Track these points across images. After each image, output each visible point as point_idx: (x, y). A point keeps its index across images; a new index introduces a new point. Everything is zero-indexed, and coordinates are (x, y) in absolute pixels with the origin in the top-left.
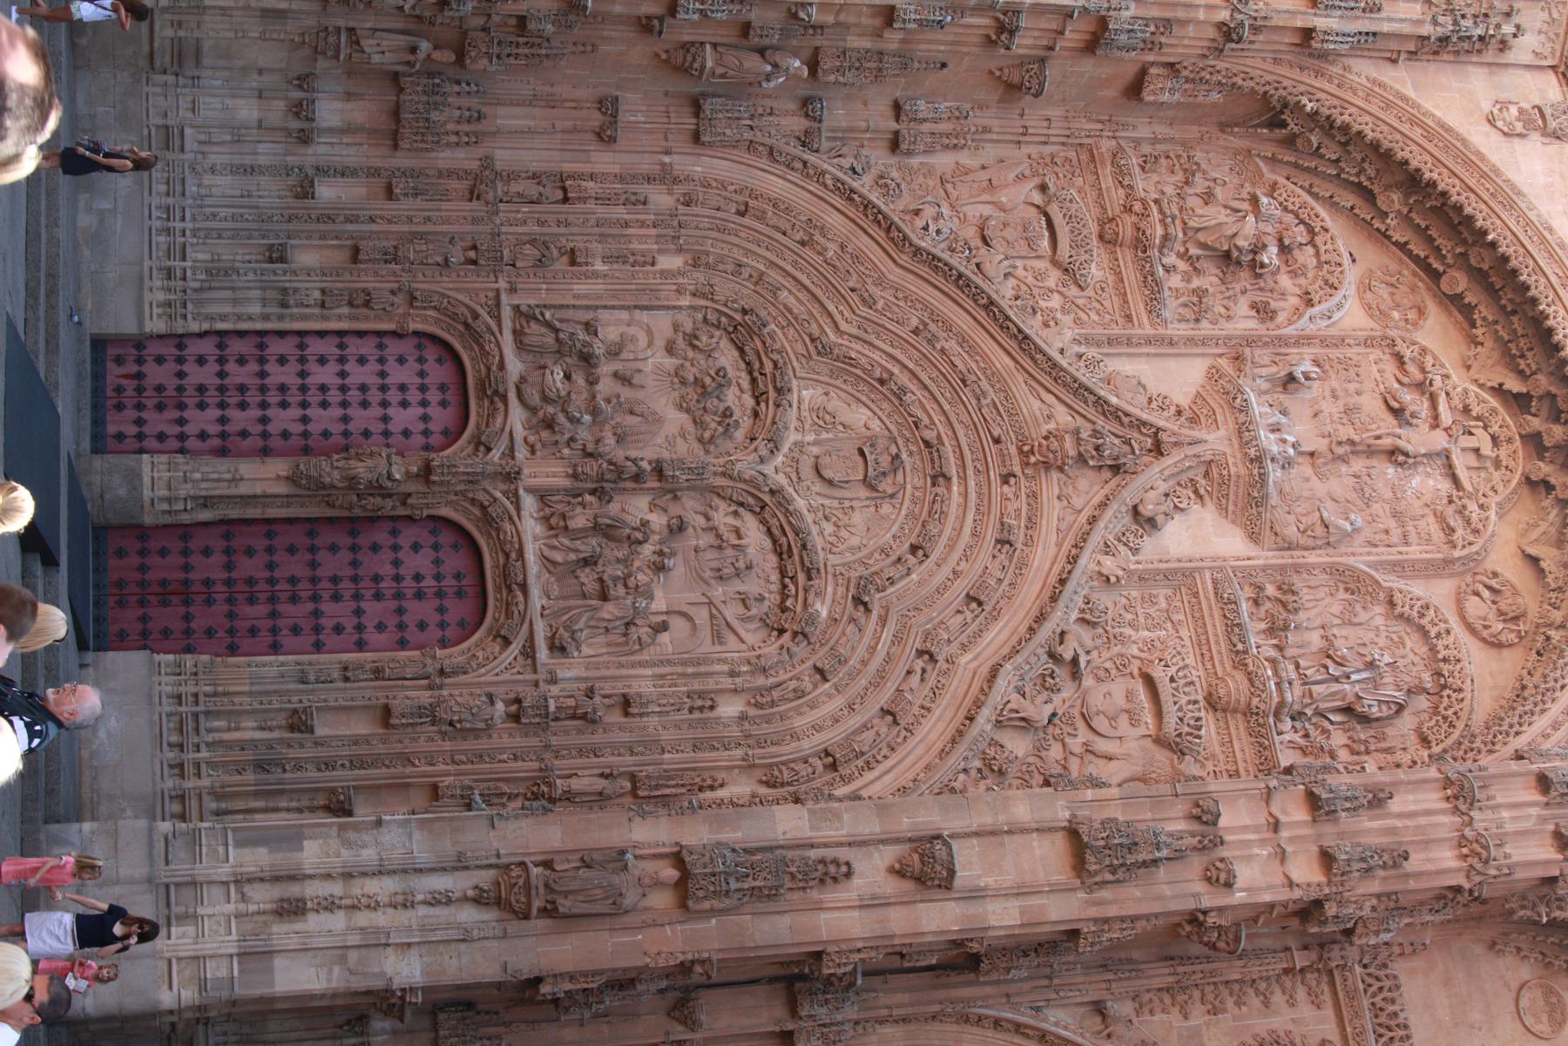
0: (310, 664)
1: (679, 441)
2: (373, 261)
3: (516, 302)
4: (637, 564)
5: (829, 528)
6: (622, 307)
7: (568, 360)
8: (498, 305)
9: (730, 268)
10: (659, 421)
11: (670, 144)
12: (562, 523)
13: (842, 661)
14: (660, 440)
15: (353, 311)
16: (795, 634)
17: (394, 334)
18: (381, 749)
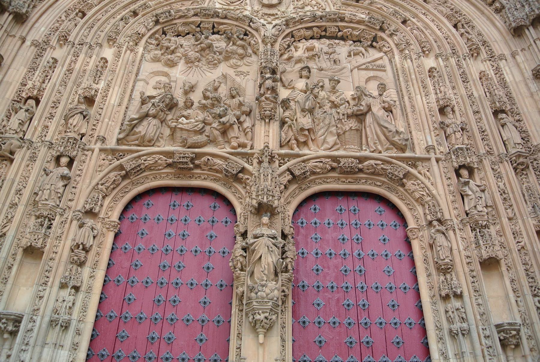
0: (439, 328)
1: (239, 69)
2: (46, 236)
3: (115, 140)
4: (333, 98)
5: (308, 8)
6: (135, 82)
7: (170, 117)
8: (113, 151)
9: (122, 23)
10: (225, 76)
11: (18, 36)
12: (306, 133)
13: (395, 14)
14: (238, 79)
15: (88, 264)
16: (382, 29)
17: (116, 236)
18: (521, 269)
